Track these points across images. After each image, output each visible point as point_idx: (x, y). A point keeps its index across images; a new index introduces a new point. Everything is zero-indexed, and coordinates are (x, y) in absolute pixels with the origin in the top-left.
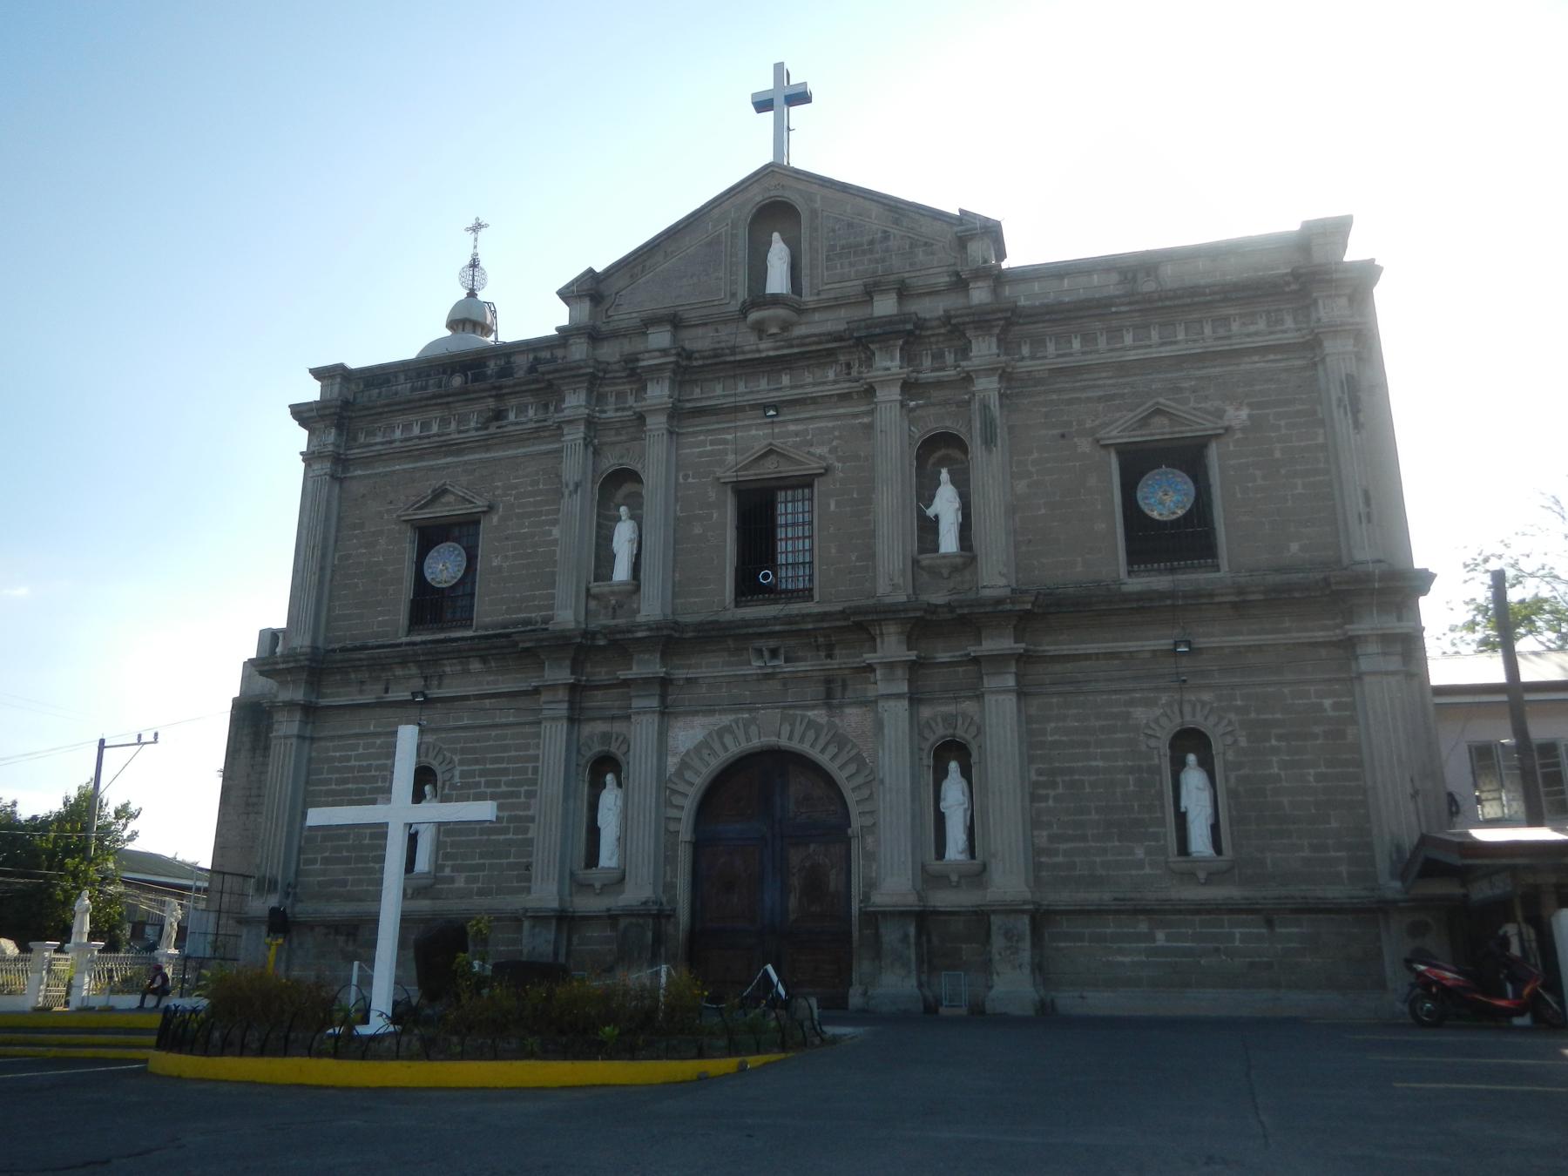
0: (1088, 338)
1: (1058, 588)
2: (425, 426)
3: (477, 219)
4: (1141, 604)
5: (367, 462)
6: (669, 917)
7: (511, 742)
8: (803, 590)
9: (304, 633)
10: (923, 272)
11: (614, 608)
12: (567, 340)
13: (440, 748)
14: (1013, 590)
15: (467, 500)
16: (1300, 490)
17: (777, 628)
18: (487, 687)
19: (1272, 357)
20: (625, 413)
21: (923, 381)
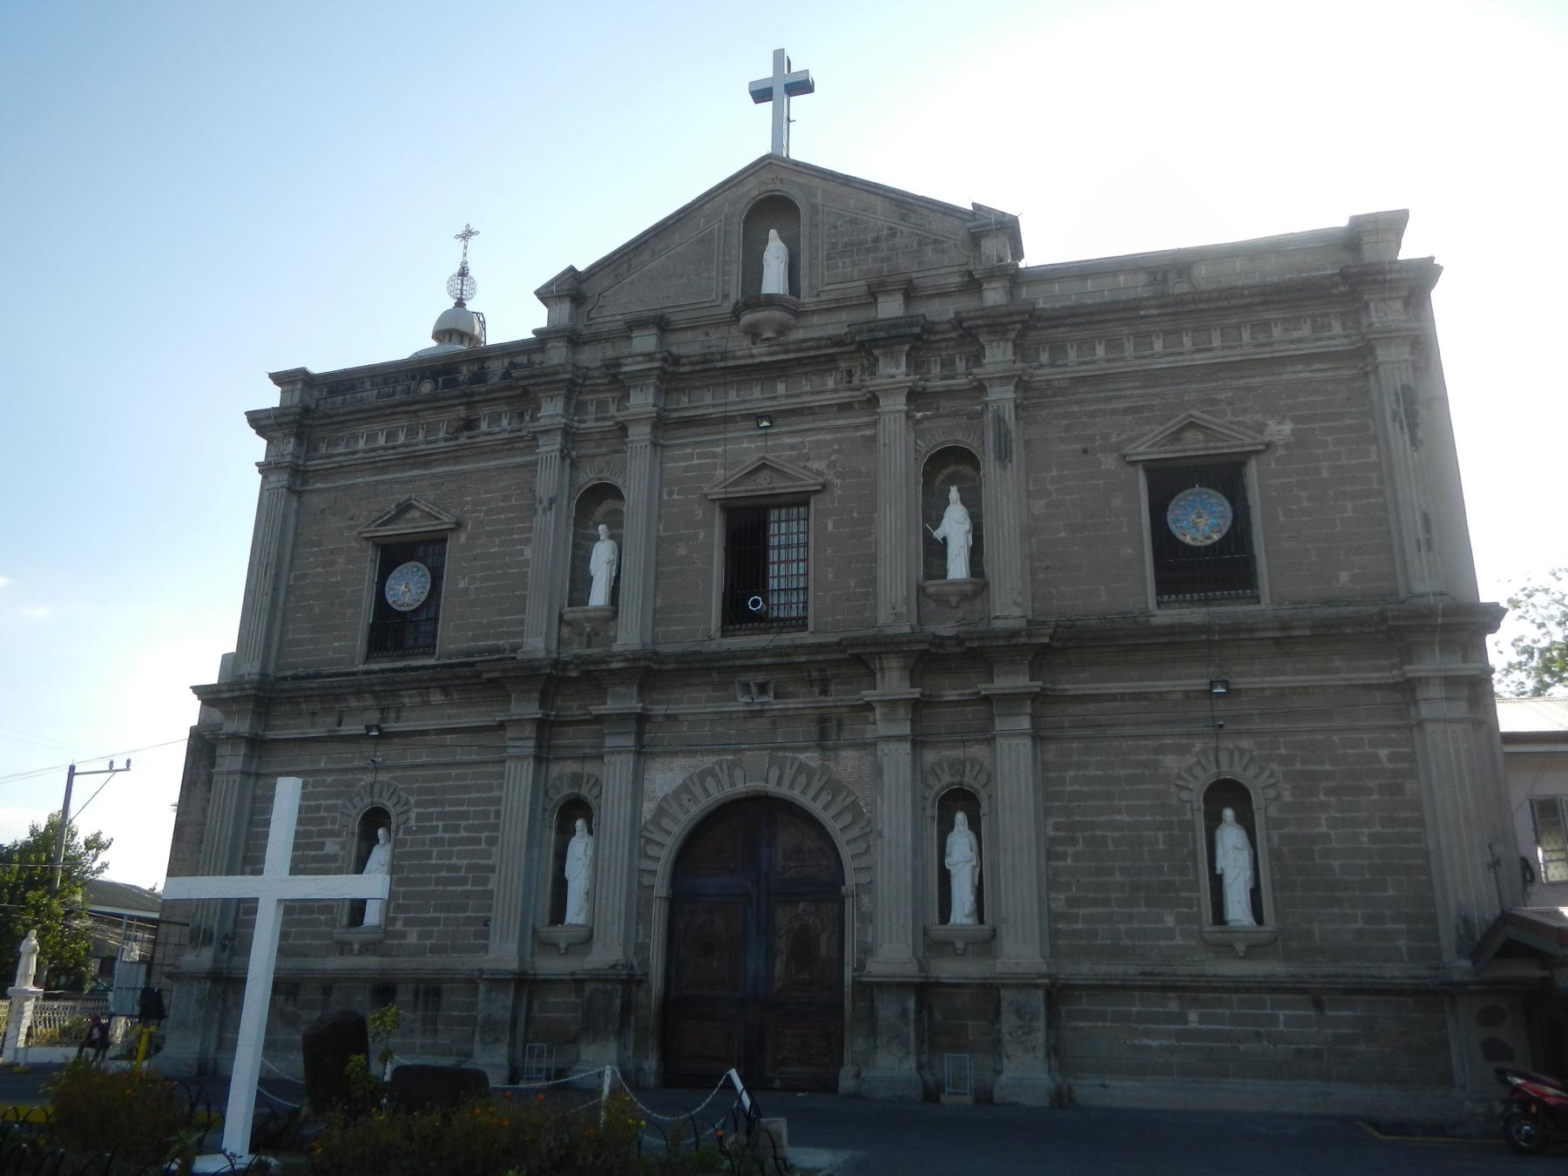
0: (1113, 344)
1: (1078, 620)
2: (391, 435)
3: (468, 226)
4: (1172, 638)
5: (326, 474)
6: (640, 982)
7: (473, 782)
8: (797, 618)
9: (253, 658)
10: (932, 273)
11: (589, 636)
12: (545, 344)
13: (396, 788)
14: (1028, 621)
15: (433, 516)
16: (1350, 514)
17: (766, 661)
18: (447, 721)
19: (1318, 366)
20: (606, 423)
21: (931, 390)
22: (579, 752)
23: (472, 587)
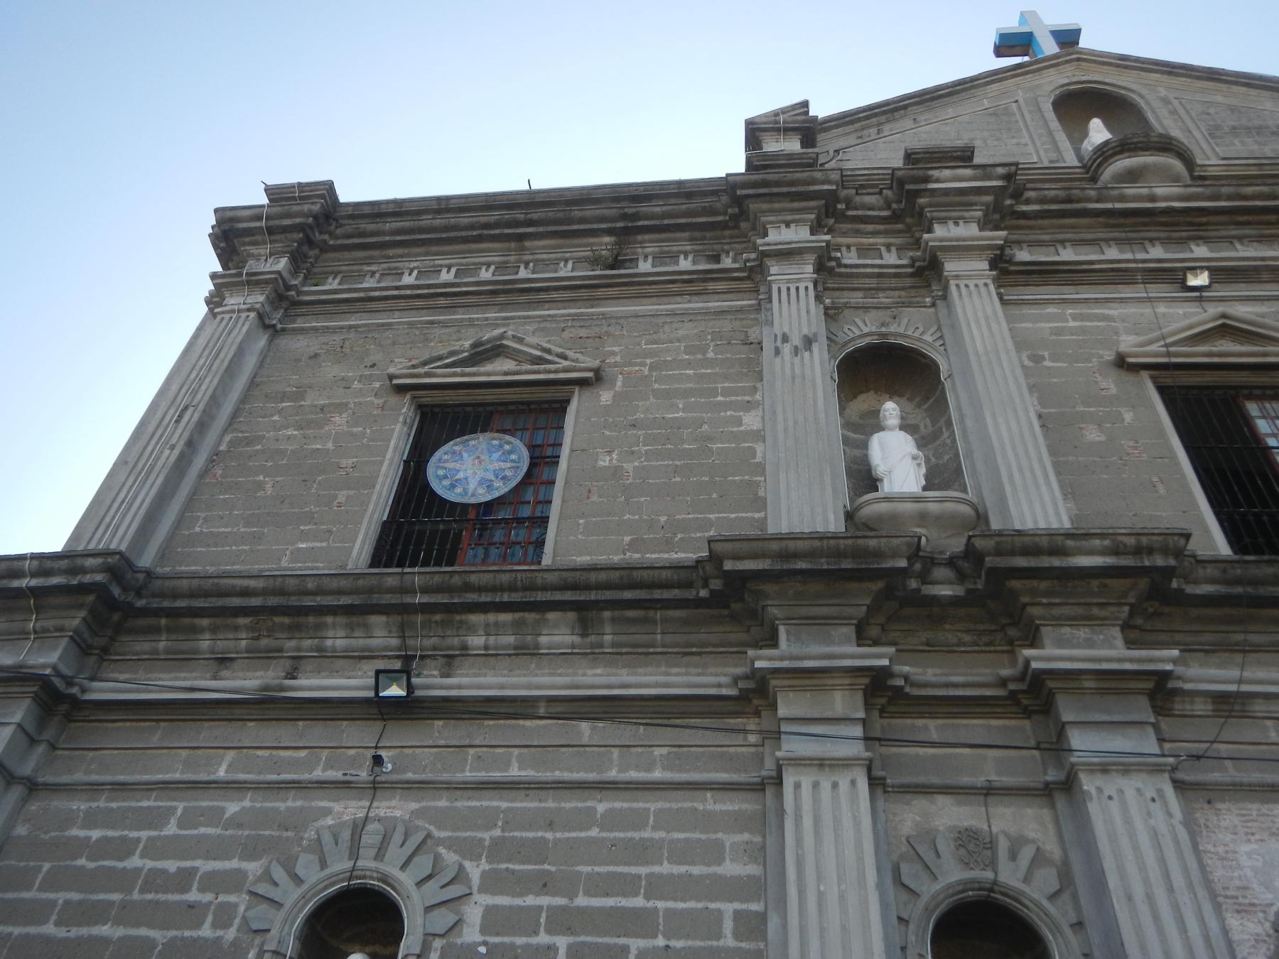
13: (429, 836)
22: (980, 781)
23: (628, 467)
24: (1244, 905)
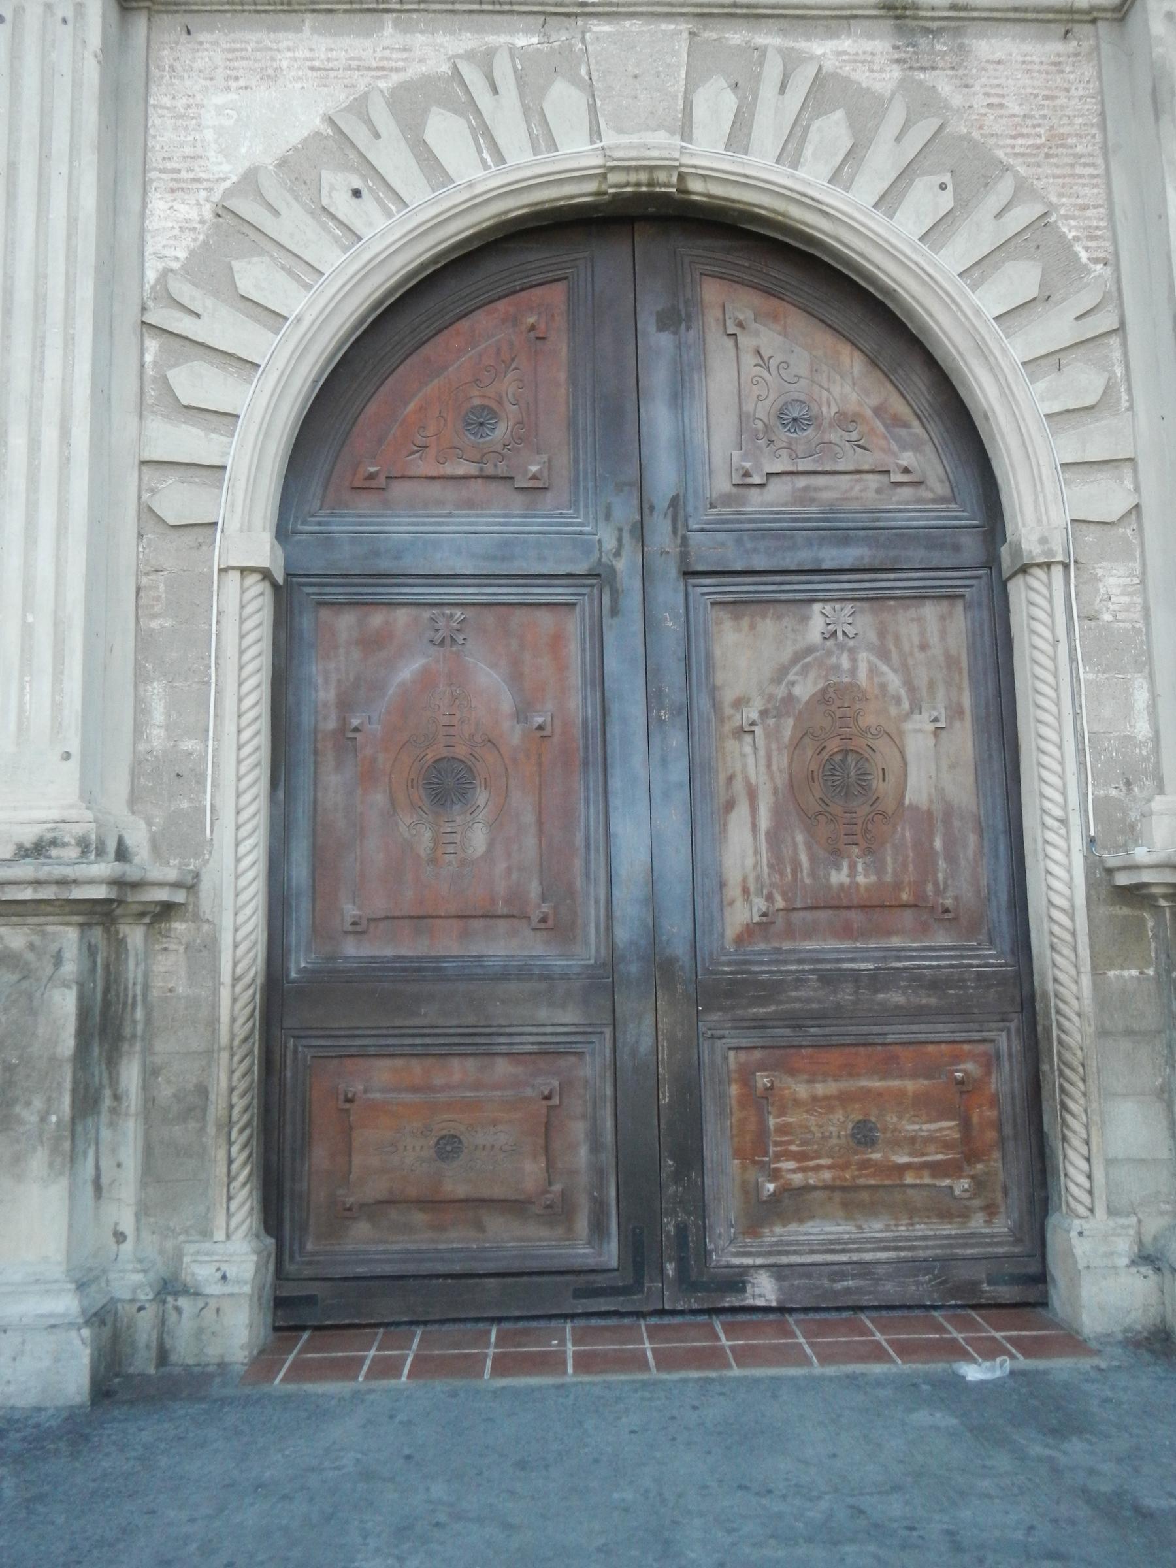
6: (167, 910)
24: (185, 181)
